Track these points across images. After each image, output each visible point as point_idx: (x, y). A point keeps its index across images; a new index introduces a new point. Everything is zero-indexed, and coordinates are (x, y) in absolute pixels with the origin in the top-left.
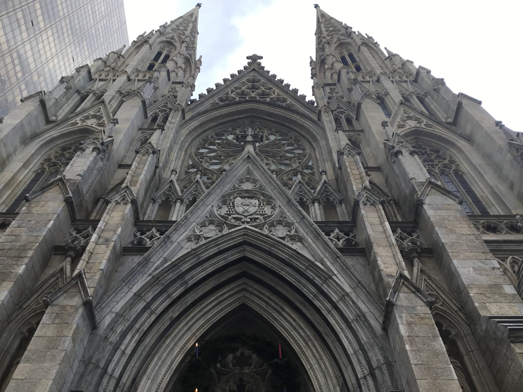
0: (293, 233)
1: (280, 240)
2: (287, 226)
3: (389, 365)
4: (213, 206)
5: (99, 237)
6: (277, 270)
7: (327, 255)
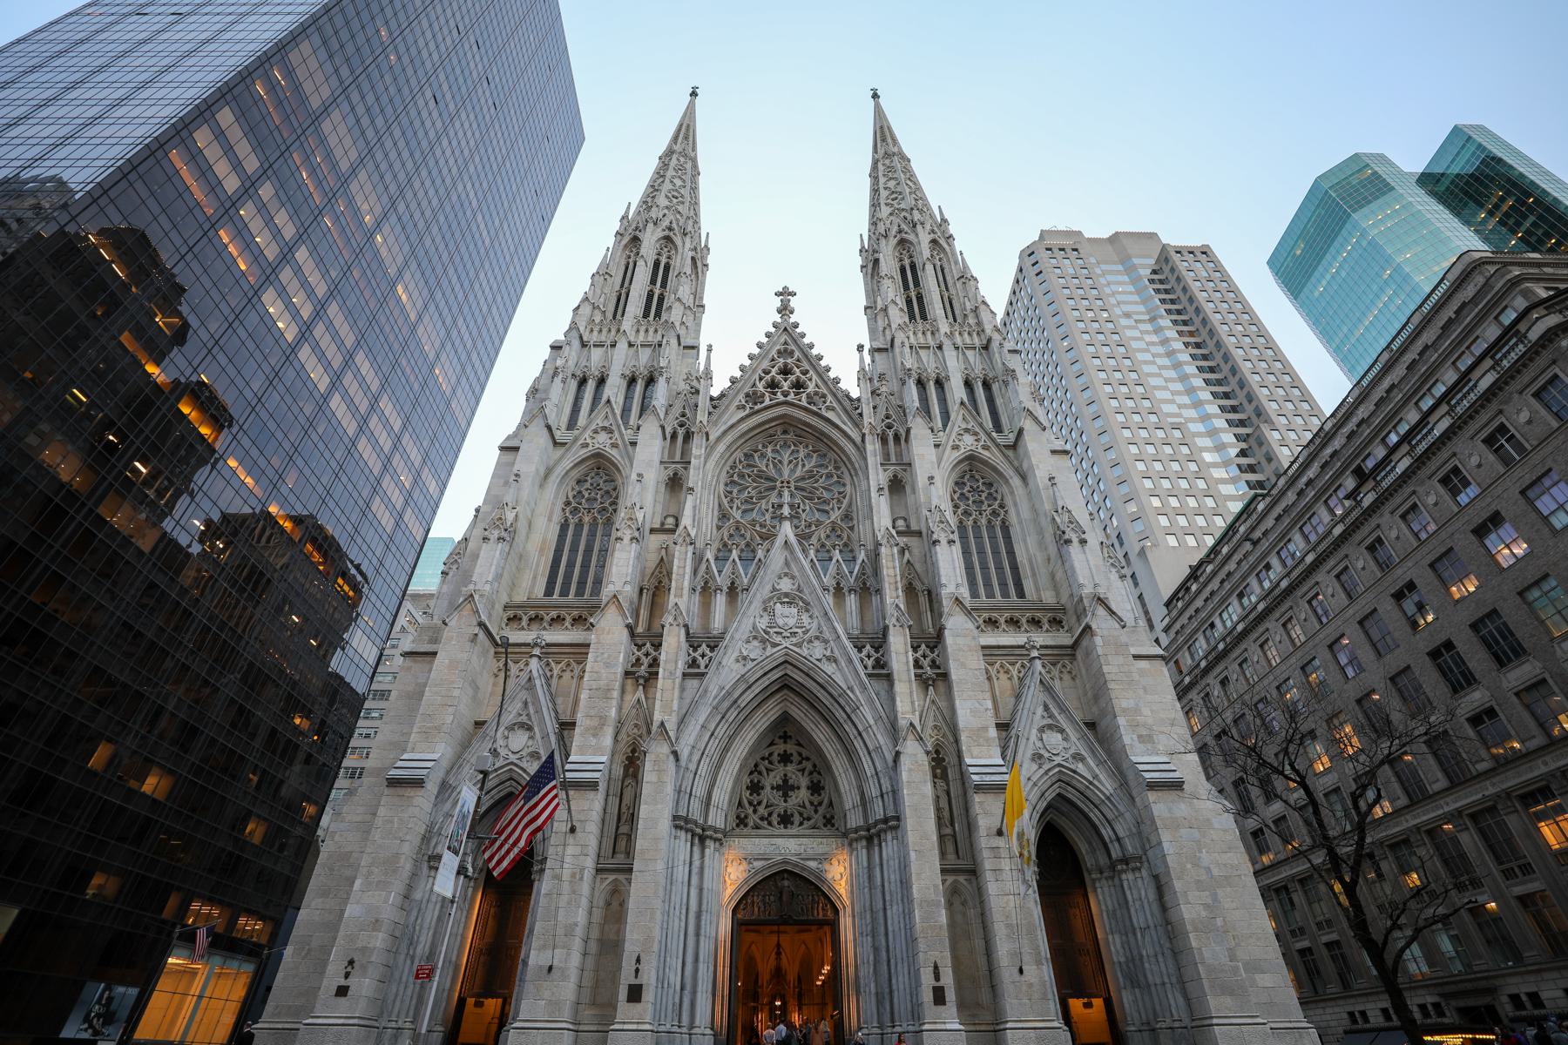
3: (895, 792)
6: (815, 692)
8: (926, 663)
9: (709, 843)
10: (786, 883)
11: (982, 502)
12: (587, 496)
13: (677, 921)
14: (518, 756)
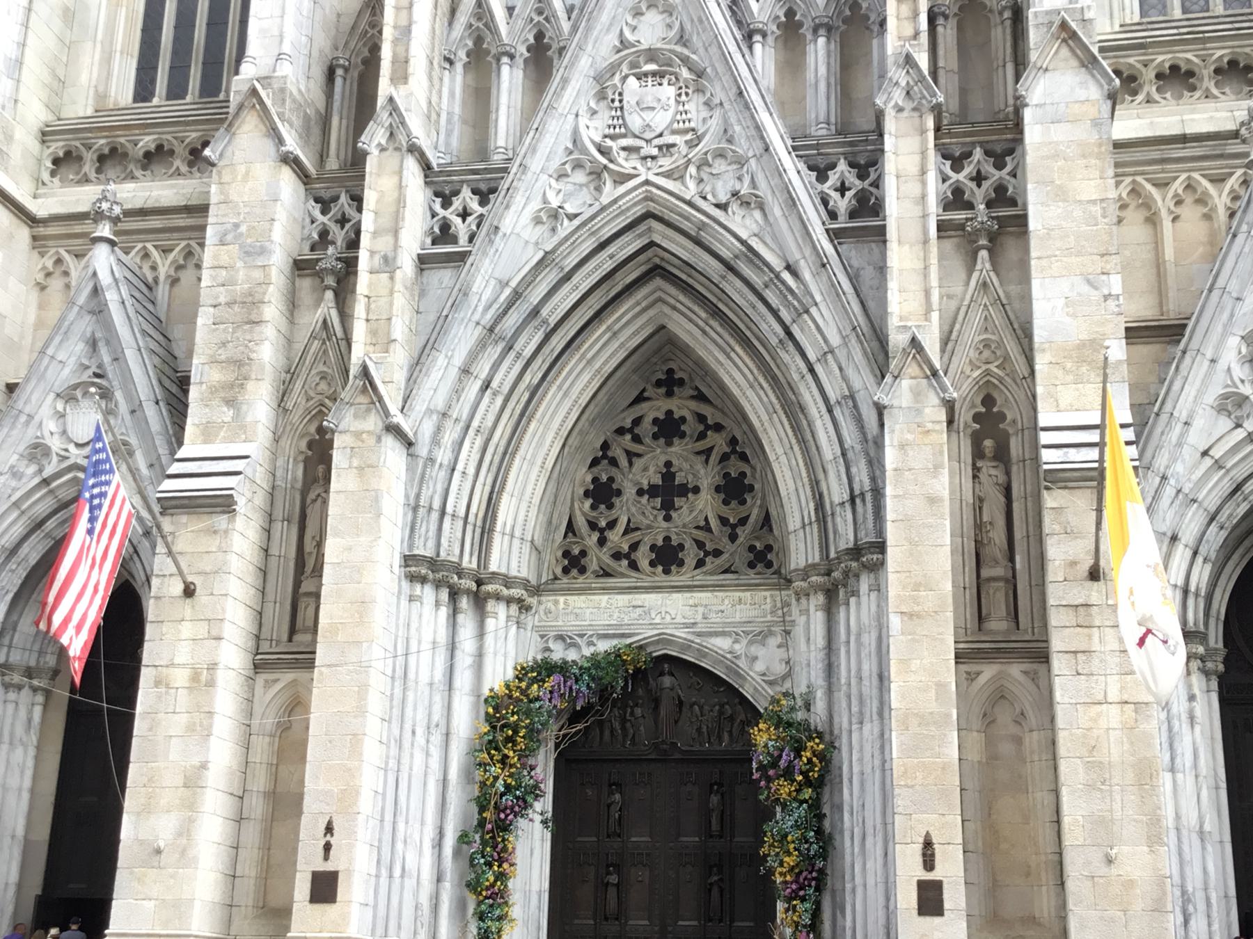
0: (745, 189)
2: (735, 162)
3: (878, 493)
4: (577, 115)
5: (372, 253)
7: (808, 252)
9: (491, 605)
10: (667, 681)
13: (419, 757)
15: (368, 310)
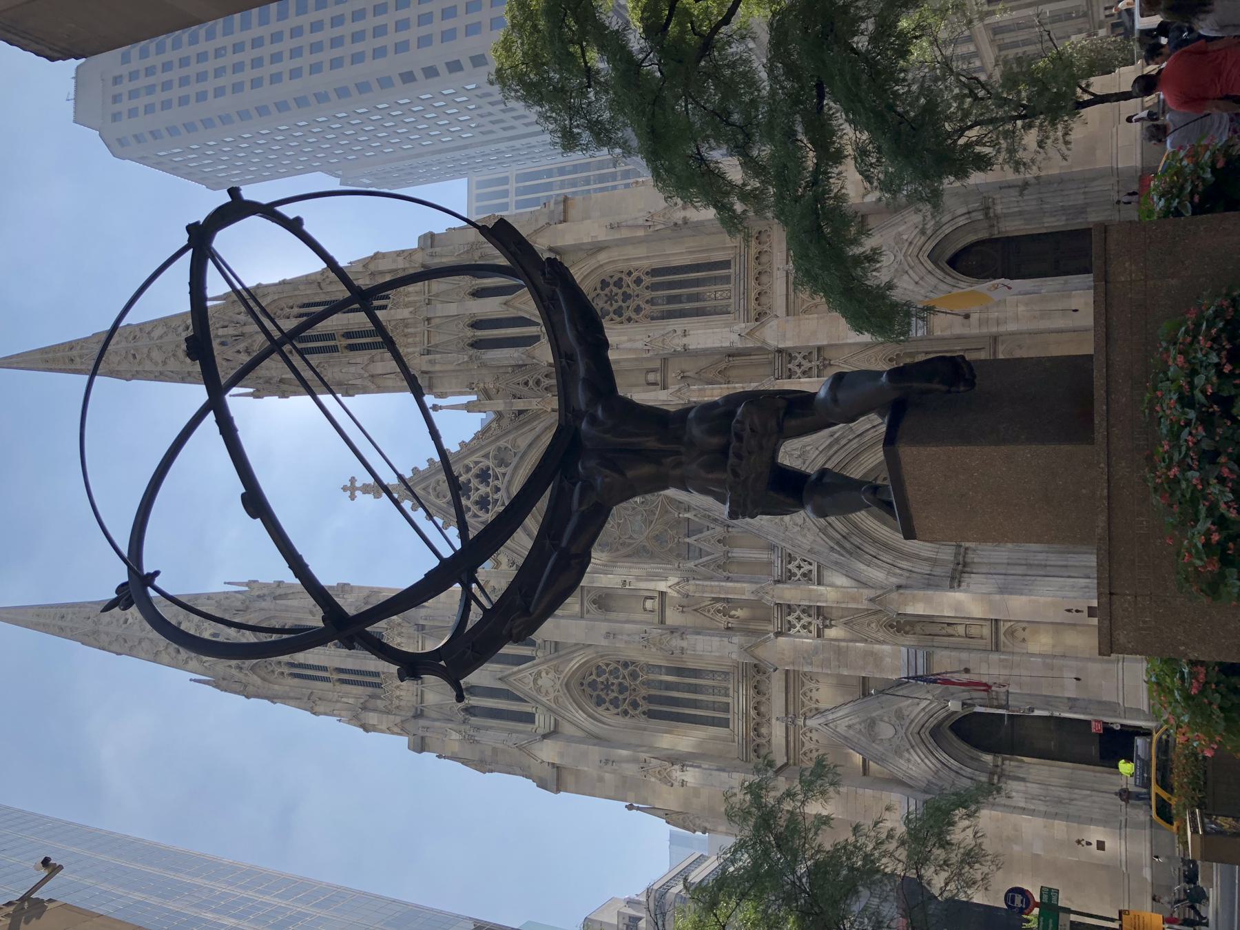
1: (807, 463)
8: (806, 365)
9: (968, 560)
11: (624, 293)
12: (616, 695)
14: (899, 728)
15: (844, 602)
